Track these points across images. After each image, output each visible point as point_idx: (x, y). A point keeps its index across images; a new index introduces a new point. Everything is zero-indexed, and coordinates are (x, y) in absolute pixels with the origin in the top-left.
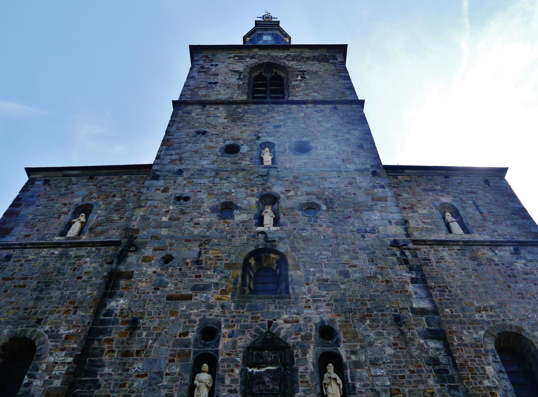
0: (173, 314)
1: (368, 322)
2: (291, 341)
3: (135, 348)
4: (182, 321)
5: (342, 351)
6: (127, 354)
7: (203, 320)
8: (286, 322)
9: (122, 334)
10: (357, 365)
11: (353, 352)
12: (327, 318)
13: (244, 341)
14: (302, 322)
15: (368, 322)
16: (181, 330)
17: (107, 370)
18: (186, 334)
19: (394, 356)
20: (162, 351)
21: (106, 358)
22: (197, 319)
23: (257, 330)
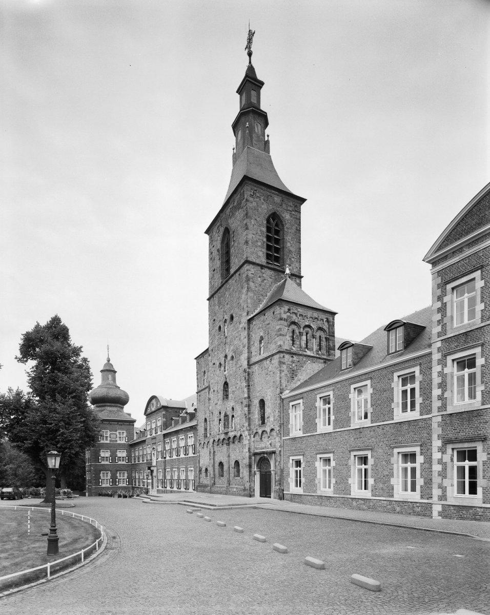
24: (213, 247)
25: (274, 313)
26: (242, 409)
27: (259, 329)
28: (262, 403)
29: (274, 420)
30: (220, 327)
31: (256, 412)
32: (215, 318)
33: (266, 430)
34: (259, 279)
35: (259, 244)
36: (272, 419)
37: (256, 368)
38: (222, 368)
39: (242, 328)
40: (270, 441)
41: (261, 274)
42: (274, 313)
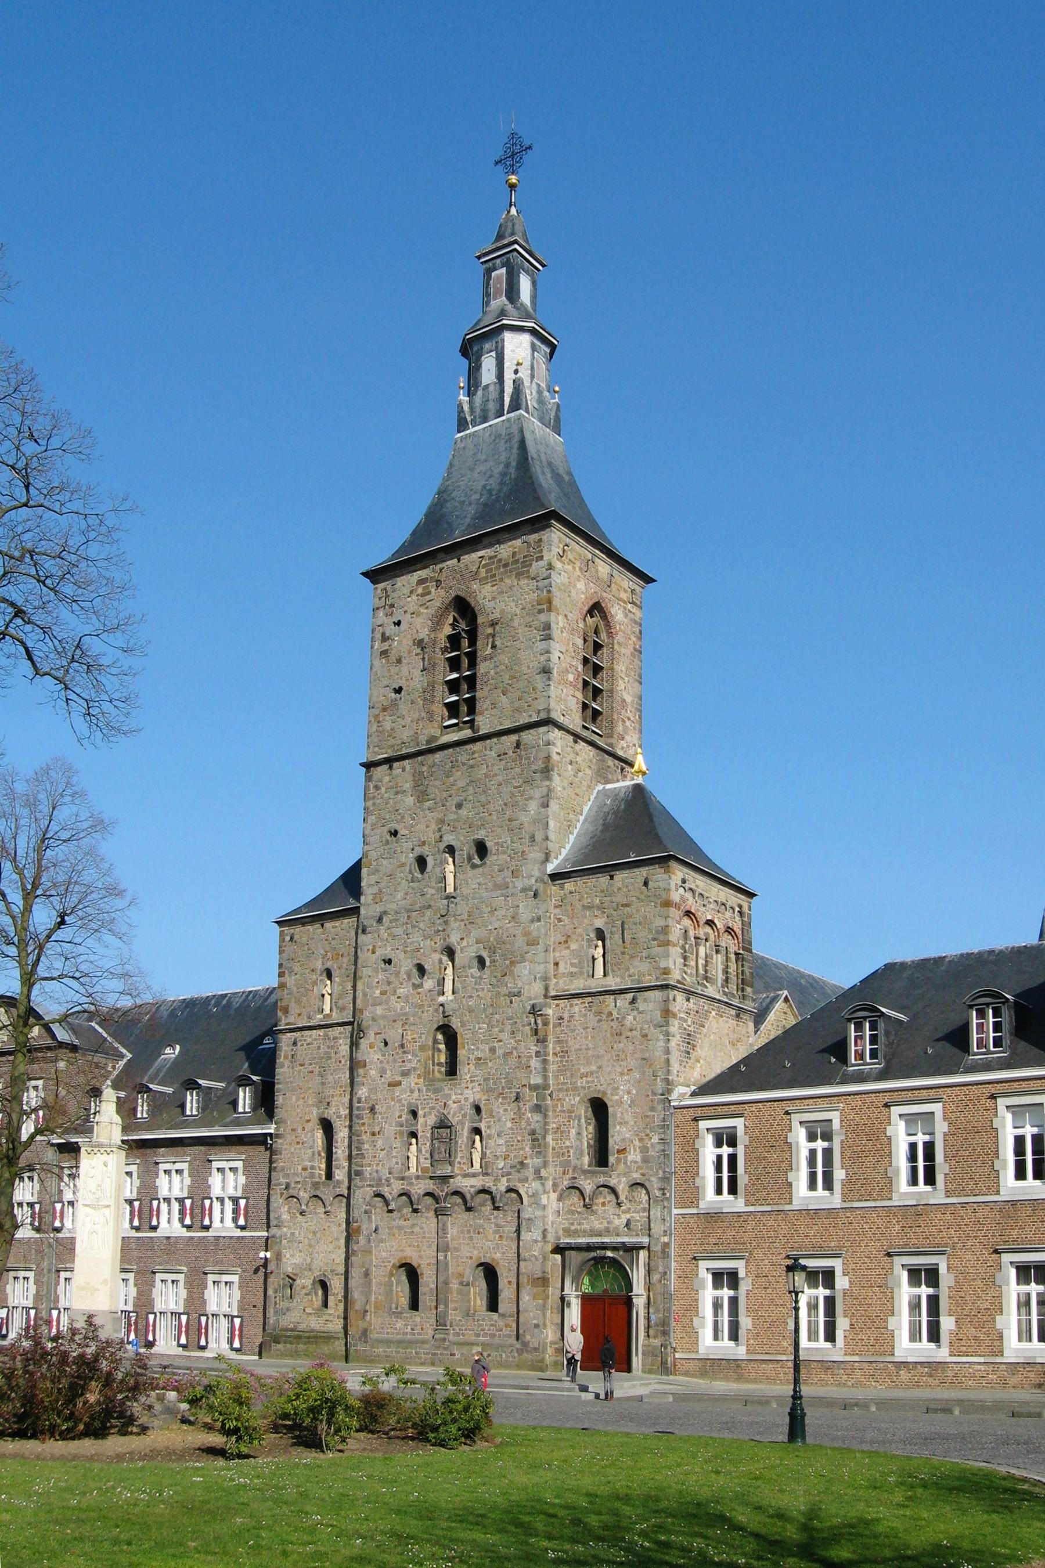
0: (393, 1099)
1: (500, 1100)
2: (454, 1121)
3: (377, 1129)
4: (398, 1105)
5: (483, 1126)
6: (373, 1134)
7: (409, 1104)
8: (454, 1102)
9: (369, 1118)
10: (490, 1137)
11: (489, 1127)
12: (477, 1097)
13: (432, 1120)
14: (463, 1102)
15: (500, 1100)
16: (397, 1114)
17: (366, 1146)
18: (400, 1117)
19: (512, 1129)
20: (390, 1129)
21: (364, 1137)
22: (405, 1103)
23: (438, 1111)
24: (398, 623)
25: (646, 884)
26: (520, 1114)
27: (588, 908)
28: (599, 1109)
29: (646, 1160)
30: (421, 862)
31: (573, 1132)
32: (394, 826)
33: (613, 1182)
34: (570, 767)
35: (571, 677)
36: (634, 1156)
37: (576, 1009)
38: (429, 983)
39: (524, 890)
40: (625, 1218)
41: (572, 756)
42: (646, 884)
